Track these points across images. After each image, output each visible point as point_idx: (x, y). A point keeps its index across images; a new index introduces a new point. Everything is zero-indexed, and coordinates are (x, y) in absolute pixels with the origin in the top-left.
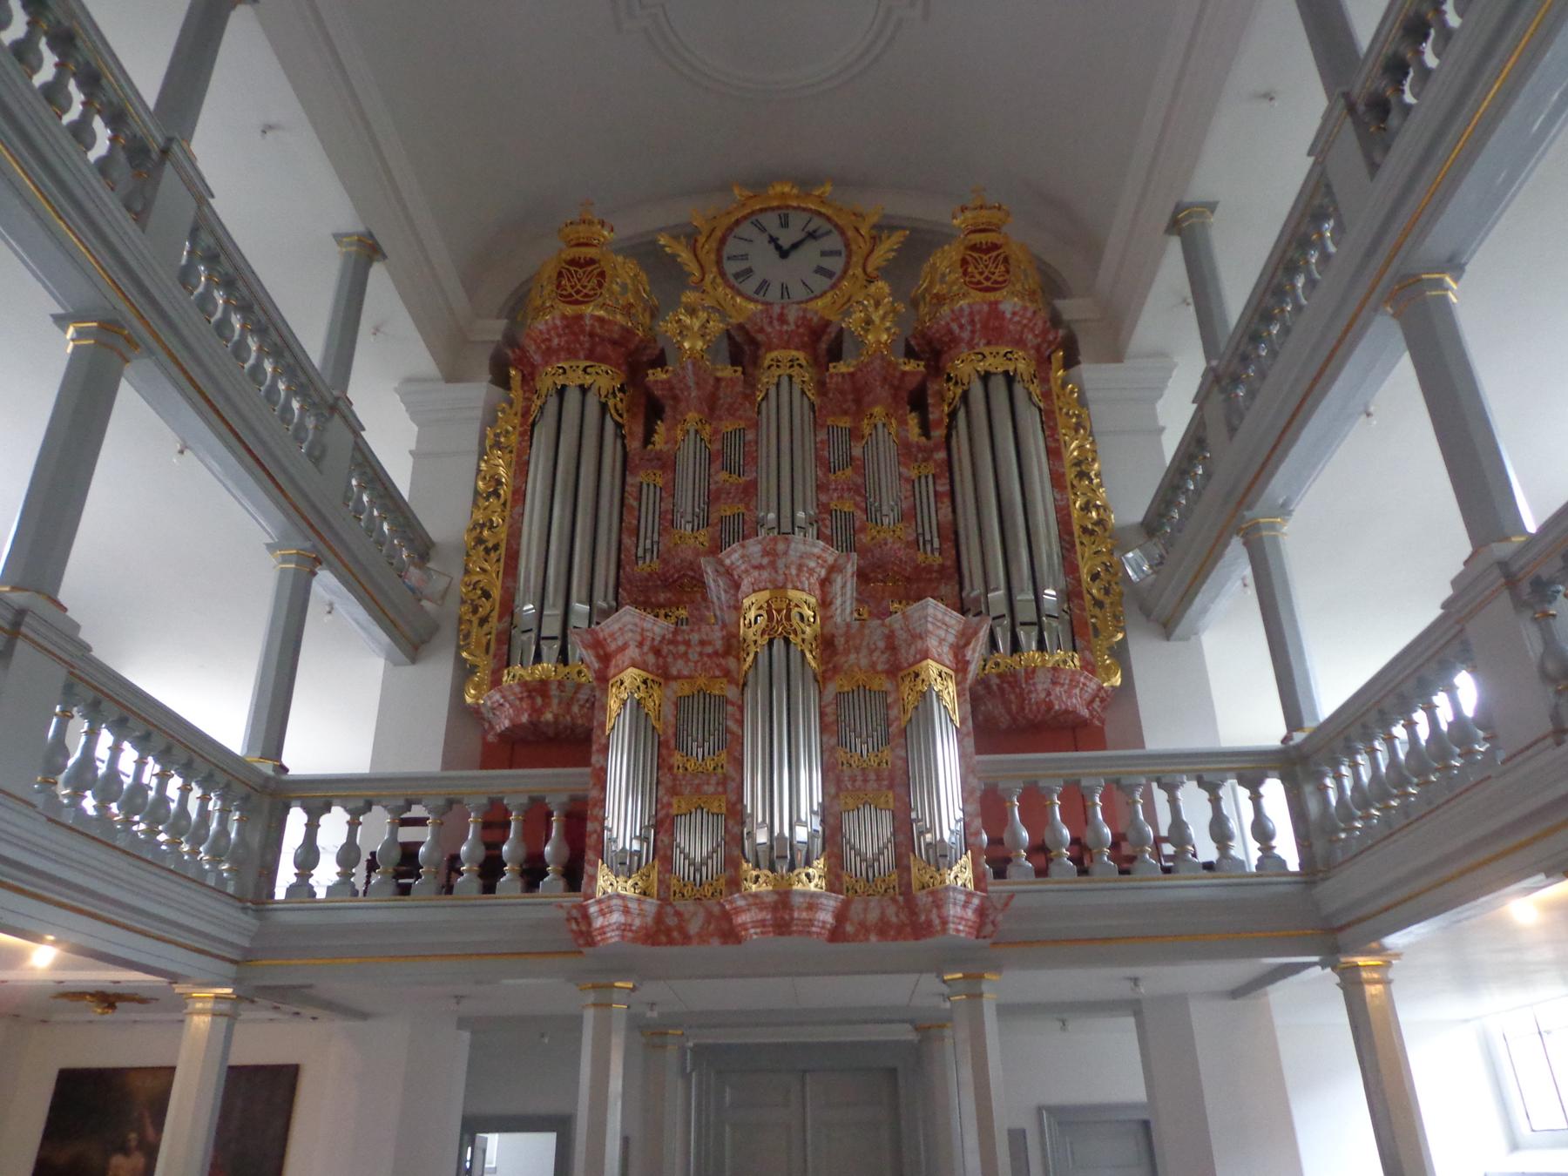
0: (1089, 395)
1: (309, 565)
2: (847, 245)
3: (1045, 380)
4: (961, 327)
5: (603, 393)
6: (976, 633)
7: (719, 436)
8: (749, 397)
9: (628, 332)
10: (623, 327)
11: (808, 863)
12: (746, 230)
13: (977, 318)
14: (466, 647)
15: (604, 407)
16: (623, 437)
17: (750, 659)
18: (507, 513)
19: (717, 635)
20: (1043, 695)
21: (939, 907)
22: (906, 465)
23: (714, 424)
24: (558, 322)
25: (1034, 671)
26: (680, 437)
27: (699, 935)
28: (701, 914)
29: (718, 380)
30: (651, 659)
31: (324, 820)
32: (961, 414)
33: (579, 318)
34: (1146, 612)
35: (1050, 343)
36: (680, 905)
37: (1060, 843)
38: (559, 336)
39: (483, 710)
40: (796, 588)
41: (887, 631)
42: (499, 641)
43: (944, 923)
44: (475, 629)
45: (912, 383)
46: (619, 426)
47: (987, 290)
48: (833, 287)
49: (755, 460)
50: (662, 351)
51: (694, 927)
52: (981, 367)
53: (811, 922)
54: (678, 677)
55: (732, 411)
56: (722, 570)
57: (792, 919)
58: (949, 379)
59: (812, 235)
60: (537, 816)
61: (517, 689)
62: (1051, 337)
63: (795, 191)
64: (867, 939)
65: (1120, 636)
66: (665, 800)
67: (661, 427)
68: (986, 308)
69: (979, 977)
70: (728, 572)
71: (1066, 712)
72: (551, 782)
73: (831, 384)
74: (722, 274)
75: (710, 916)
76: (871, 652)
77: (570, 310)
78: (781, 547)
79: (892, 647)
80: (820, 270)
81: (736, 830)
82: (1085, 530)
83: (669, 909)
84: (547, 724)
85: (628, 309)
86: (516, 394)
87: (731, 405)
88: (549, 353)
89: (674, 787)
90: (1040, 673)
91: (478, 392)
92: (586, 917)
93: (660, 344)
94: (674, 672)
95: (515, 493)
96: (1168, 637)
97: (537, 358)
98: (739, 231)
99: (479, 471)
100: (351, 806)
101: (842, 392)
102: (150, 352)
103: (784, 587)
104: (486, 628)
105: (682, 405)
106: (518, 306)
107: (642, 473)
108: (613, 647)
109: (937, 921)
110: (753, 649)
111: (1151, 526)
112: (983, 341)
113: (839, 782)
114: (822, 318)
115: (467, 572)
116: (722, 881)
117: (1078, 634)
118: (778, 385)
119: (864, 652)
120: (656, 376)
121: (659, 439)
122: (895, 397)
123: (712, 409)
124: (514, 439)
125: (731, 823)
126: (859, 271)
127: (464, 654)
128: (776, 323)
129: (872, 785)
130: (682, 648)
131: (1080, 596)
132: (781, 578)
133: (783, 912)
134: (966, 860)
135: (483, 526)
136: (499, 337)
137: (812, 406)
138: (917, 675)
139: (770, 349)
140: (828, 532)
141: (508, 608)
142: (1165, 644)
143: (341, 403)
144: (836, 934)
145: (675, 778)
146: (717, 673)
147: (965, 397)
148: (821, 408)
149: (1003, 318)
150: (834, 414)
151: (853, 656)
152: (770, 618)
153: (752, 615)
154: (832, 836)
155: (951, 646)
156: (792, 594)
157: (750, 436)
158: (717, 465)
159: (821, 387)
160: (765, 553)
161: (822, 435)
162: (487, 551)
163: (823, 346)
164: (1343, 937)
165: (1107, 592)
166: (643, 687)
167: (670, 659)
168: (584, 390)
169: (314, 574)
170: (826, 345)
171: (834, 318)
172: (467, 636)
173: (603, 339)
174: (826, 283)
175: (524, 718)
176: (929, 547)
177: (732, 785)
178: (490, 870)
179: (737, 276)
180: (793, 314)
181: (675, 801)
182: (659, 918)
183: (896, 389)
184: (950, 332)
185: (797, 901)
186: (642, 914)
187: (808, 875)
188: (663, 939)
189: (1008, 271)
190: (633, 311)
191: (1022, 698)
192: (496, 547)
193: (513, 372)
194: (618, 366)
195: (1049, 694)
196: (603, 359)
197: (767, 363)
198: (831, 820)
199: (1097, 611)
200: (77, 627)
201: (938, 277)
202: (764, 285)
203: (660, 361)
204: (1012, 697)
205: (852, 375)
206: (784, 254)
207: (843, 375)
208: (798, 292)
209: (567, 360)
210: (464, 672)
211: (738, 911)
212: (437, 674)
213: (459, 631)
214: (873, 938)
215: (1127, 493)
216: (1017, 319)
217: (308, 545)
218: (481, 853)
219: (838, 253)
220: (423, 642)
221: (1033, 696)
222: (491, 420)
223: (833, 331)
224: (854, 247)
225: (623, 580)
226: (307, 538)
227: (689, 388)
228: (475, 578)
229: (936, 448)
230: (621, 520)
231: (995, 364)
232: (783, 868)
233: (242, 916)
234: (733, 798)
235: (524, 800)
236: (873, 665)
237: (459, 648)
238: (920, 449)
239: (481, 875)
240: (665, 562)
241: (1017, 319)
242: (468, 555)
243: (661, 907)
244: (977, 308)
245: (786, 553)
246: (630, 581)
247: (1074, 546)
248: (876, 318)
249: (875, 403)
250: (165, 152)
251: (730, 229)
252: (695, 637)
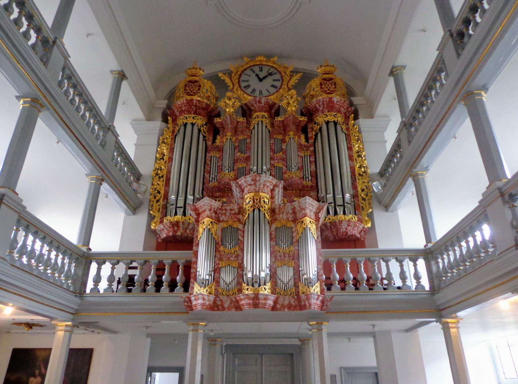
0: (362, 129)
1: (100, 181)
2: (282, 77)
3: (347, 124)
4: (320, 106)
5: (199, 125)
6: (322, 208)
7: (238, 141)
8: (248, 128)
9: (208, 106)
10: (206, 104)
11: (265, 284)
12: (248, 72)
13: (325, 103)
14: (152, 210)
15: (199, 130)
16: (206, 141)
17: (247, 215)
18: (166, 165)
19: (236, 208)
20: (344, 230)
21: (308, 300)
22: (300, 152)
23: (236, 136)
24: (185, 102)
25: (342, 221)
26: (225, 141)
27: (228, 308)
28: (229, 301)
29: (238, 122)
30: (214, 215)
31: (103, 267)
32: (319, 135)
33: (192, 100)
34: (380, 203)
35: (349, 112)
36: (222, 297)
37: (349, 279)
38: (185, 106)
39: (157, 231)
40: (262, 192)
41: (293, 207)
42: (163, 208)
43: (310, 305)
44: (155, 204)
45: (302, 124)
46: (204, 137)
47: (328, 93)
48: (277, 91)
49: (250, 149)
50: (219, 112)
51: (226, 305)
52: (326, 119)
53: (265, 304)
54: (222, 221)
55: (242, 132)
56: (238, 185)
57: (259, 303)
58: (315, 123)
59: (270, 74)
60: (174, 266)
61: (169, 224)
62: (349, 110)
63: (265, 59)
64: (284, 310)
65: (371, 210)
66: (217, 262)
67: (218, 137)
68: (328, 100)
69: (321, 324)
70: (240, 186)
71: (352, 235)
72: (180, 256)
73: (276, 124)
74: (240, 86)
75: (232, 301)
76: (287, 214)
77: (189, 98)
78: (258, 178)
79: (294, 213)
80: (273, 86)
81: (241, 273)
82: (360, 174)
83: (218, 299)
84: (178, 236)
85: (208, 98)
86: (170, 125)
87: (242, 130)
88: (182, 112)
89: (221, 258)
90: (344, 222)
91: (158, 124)
92: (190, 301)
93: (219, 109)
94: (221, 219)
95: (169, 158)
96: (387, 211)
97: (177, 113)
98: (246, 72)
99: (157, 151)
100: (112, 262)
101: (279, 127)
102: (48, 109)
103: (259, 192)
104: (159, 203)
105: (226, 130)
106: (171, 96)
107: (212, 153)
108: (201, 211)
109: (308, 305)
110: (248, 212)
111: (382, 174)
112: (327, 111)
113: (276, 257)
114: (273, 102)
115: (153, 184)
116: (236, 290)
117: (357, 209)
118: (258, 124)
119: (285, 214)
120: (217, 120)
121: (218, 141)
122: (297, 129)
123: (236, 132)
124: (169, 140)
125: (239, 270)
126: (286, 86)
127: (151, 212)
128: (257, 103)
129: (287, 258)
130: (224, 212)
131: (357, 196)
132: (258, 189)
133: (256, 301)
134: (318, 284)
135: (158, 169)
136: (165, 106)
137: (269, 131)
138: (302, 222)
139: (255, 112)
140: (274, 173)
141: (166, 197)
142: (386, 213)
143: (111, 127)
144: (274, 308)
145: (221, 255)
146: (236, 220)
147: (320, 129)
148: (272, 132)
149: (334, 103)
150: (276, 134)
151: (281, 215)
152: (254, 202)
153: (248, 201)
154: (273, 275)
155: (314, 212)
156: (261, 194)
157: (248, 141)
158: (237, 151)
159: (272, 125)
160: (253, 180)
161: (272, 141)
162: (159, 178)
163: (273, 111)
164: (443, 312)
165: (367, 195)
166: (211, 224)
167: (220, 215)
168: (193, 124)
169: (101, 184)
170: (274, 110)
171: (277, 102)
172: (152, 206)
173: (199, 108)
174: (275, 90)
175: (171, 234)
176: (307, 179)
177: (240, 258)
178: (158, 285)
179: (245, 87)
180: (263, 100)
181: (221, 262)
182: (215, 302)
183: (297, 126)
184: (316, 107)
185: (261, 297)
186: (209, 300)
187: (265, 288)
188: (216, 309)
189: (335, 87)
190: (210, 98)
191: (337, 230)
192: (162, 176)
193: (169, 118)
194: (204, 117)
195: (346, 229)
196: (200, 114)
197: (254, 117)
198: (273, 270)
199: (363, 202)
200: (22, 200)
201: (312, 89)
202: (254, 90)
203: (219, 115)
204: (334, 230)
205: (283, 121)
206: (261, 80)
207: (280, 121)
208: (265, 93)
209: (187, 114)
210: (151, 218)
211: (241, 300)
212: (142, 218)
213: (150, 204)
214: (286, 310)
215: (374, 163)
216: (338, 103)
217: (100, 174)
218: (155, 279)
219: (279, 80)
220: (138, 208)
221: (341, 230)
223: (277, 106)
224: (284, 78)
225: (205, 188)
226: (99, 172)
227: (228, 124)
228: (155, 187)
229: (311, 146)
230: (205, 168)
231: (331, 118)
232: (256, 285)
233: (75, 298)
234: (240, 262)
235: (170, 261)
236: (288, 218)
237: (149, 210)
238: (305, 146)
239: (155, 286)
240: (219, 183)
241: (338, 103)
242: (153, 179)
243: (215, 298)
244: (325, 99)
245: (259, 180)
246: (207, 189)
247: (356, 180)
248: (291, 102)
249: (290, 131)
250: (54, 42)
251: (243, 72)
252: (228, 208)
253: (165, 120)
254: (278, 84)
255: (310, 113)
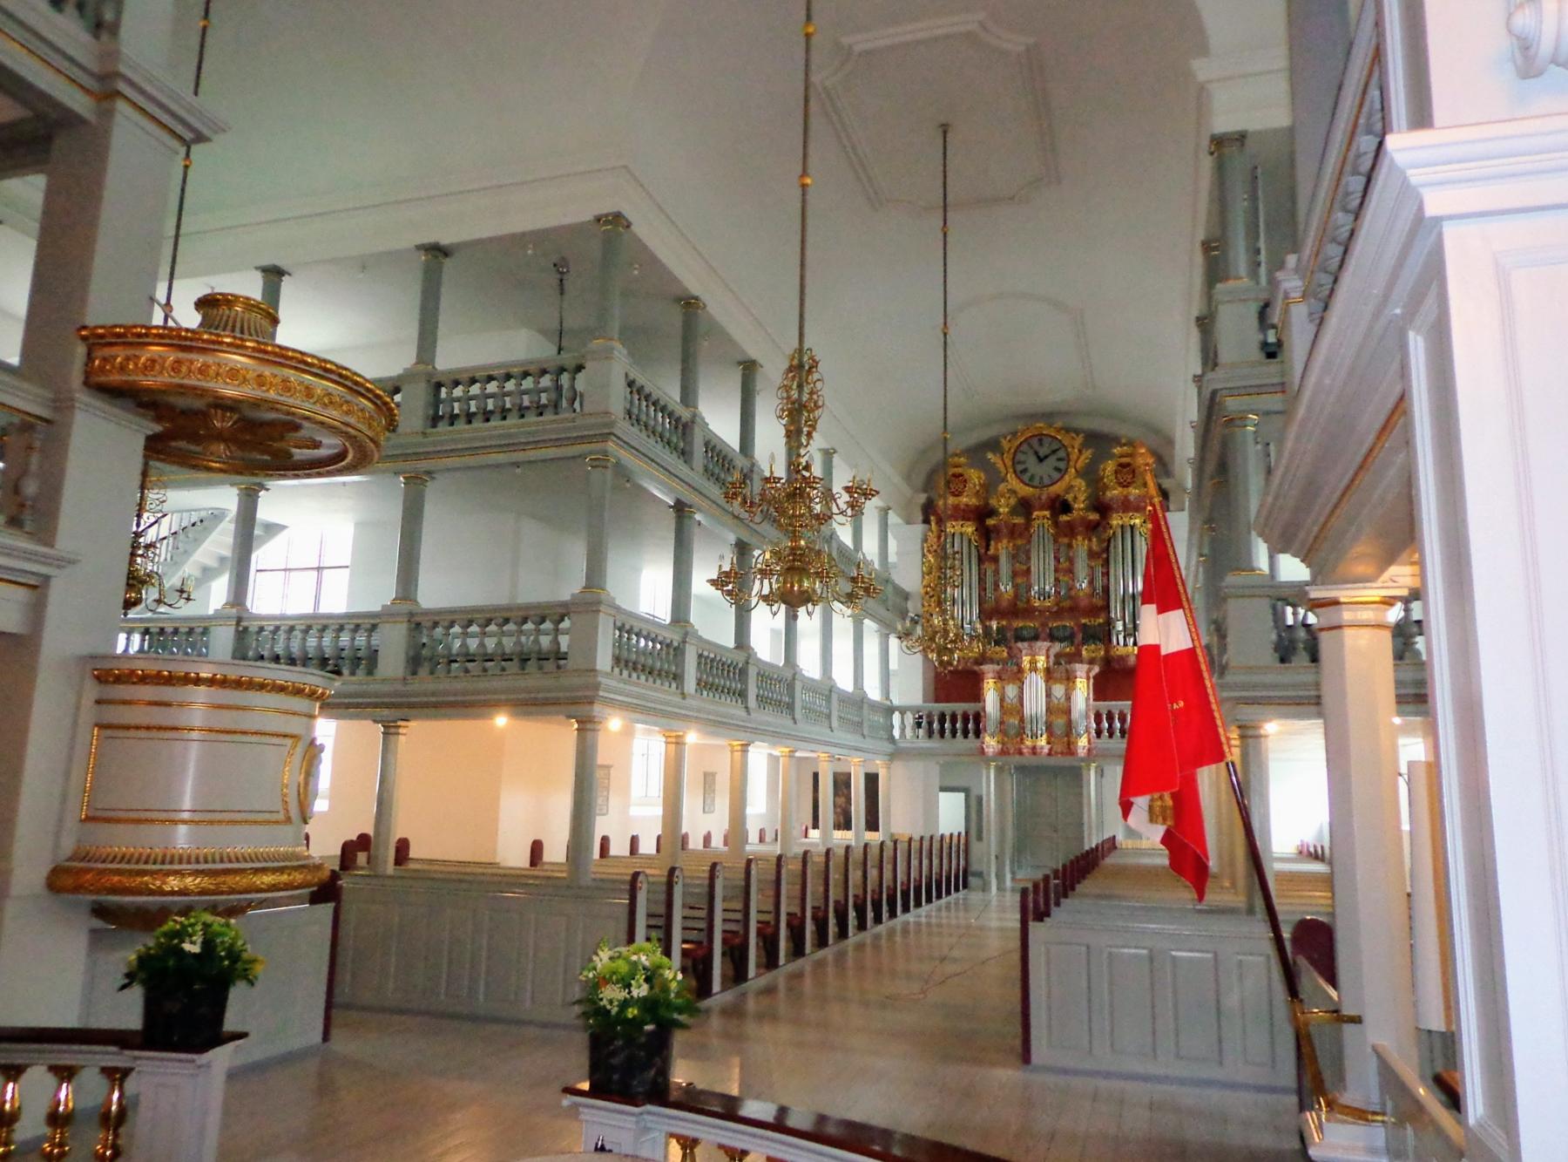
12: (1025, 447)
55: (1021, 535)
59: (1054, 452)
91: (919, 529)
106: (928, 485)
120: (991, 522)
121: (992, 552)
144: (1049, 754)
159: (1056, 524)
170: (1060, 506)
178: (954, 734)
180: (1044, 497)
206: (1041, 460)
222: (925, 540)
253: (926, 521)
254: (1062, 465)
255: (1103, 508)
